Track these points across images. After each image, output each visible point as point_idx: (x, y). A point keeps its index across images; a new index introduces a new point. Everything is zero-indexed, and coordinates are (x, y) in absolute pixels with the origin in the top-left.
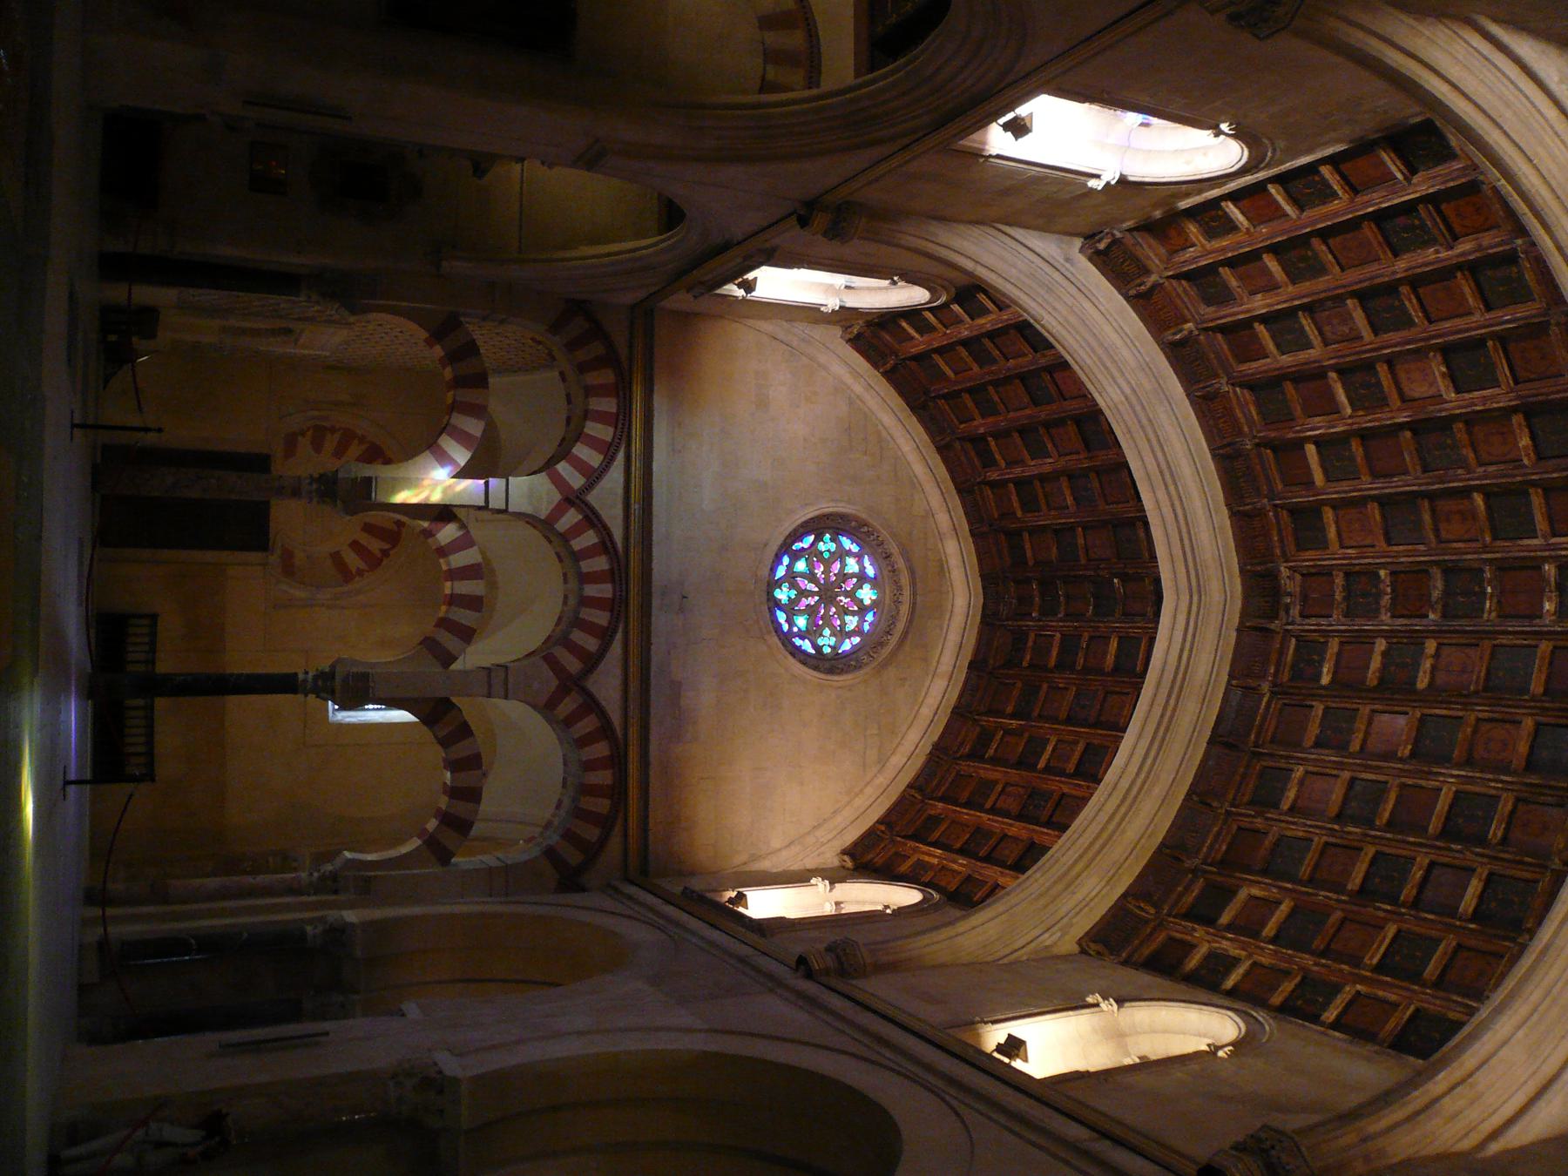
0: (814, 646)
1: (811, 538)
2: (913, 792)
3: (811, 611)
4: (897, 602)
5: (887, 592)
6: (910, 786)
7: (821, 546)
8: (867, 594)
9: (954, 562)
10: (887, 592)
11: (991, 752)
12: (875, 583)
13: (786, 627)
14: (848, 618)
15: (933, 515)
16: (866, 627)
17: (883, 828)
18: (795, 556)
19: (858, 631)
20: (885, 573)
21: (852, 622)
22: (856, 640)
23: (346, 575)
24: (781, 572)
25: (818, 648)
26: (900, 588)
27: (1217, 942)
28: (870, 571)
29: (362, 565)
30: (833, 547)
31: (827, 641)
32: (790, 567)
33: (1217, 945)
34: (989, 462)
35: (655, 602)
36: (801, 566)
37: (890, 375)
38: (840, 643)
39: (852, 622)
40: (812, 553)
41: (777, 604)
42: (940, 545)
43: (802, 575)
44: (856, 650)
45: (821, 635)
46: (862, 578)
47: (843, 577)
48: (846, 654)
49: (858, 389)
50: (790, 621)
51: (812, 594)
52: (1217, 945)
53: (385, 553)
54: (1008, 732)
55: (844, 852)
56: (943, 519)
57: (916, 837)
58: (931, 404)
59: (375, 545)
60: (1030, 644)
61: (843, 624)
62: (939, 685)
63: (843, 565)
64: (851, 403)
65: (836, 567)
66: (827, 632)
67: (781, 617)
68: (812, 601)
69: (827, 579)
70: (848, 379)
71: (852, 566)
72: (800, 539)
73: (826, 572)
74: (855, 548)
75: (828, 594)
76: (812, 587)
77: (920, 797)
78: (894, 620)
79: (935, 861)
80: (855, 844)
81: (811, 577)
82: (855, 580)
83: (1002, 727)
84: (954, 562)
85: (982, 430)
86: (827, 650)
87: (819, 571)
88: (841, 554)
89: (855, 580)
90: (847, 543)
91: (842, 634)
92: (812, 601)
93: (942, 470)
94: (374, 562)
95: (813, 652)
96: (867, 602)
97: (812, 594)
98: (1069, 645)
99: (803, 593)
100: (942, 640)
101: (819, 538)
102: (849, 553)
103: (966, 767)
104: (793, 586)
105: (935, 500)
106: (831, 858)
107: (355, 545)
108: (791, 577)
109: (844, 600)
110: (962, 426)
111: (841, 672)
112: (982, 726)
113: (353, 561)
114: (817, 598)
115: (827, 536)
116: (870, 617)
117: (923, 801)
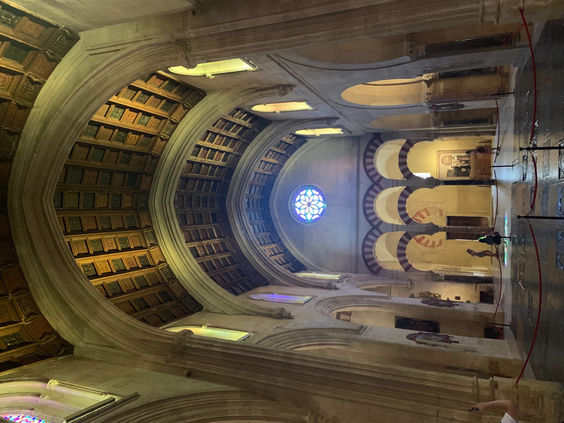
9: (276, 213)
11: (271, 166)
16: (299, 196)
22: (301, 193)
23: (425, 210)
28: (297, 210)
29: (421, 212)
34: (270, 236)
53: (416, 216)
54: (267, 170)
55: (307, 141)
56: (279, 223)
57: (290, 145)
59: (418, 217)
62: (281, 182)
64: (304, 252)
74: (302, 216)
78: (292, 199)
79: (288, 140)
80: (304, 143)
83: (268, 172)
84: (276, 213)
93: (280, 235)
94: (418, 213)
103: (276, 162)
105: (281, 228)
106: (310, 141)
107: (423, 218)
113: (424, 213)
114: (312, 203)
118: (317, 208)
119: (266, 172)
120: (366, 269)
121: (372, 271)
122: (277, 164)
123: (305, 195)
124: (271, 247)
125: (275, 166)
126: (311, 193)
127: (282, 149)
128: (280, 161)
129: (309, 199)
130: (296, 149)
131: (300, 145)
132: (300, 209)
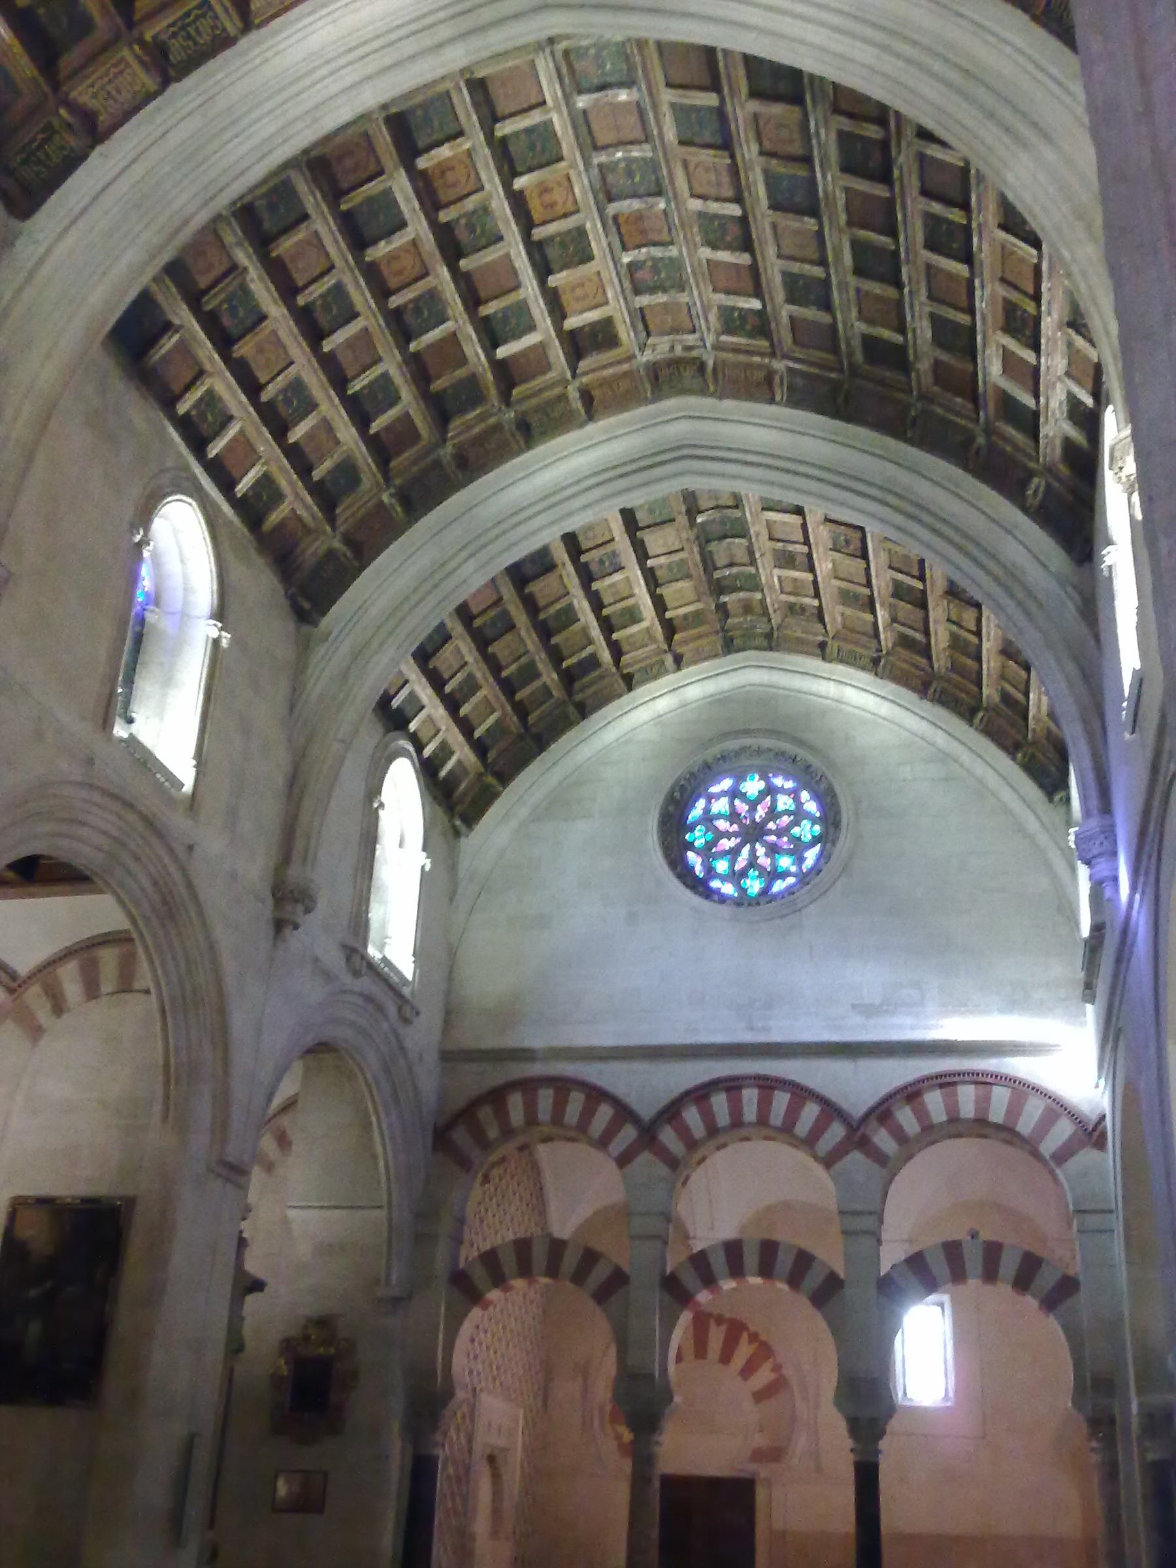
0: (812, 844)
1: (691, 855)
2: (977, 721)
3: (773, 850)
4: (759, 751)
5: (748, 763)
6: (970, 722)
7: (699, 843)
8: (753, 786)
10: (748, 763)
11: (919, 636)
12: (740, 778)
13: (791, 880)
14: (781, 807)
15: (660, 716)
16: (789, 785)
17: (1019, 755)
18: (710, 872)
19: (794, 794)
20: (726, 766)
21: (784, 802)
22: (805, 795)
24: (728, 889)
25: (816, 840)
26: (743, 749)
27: (1053, 413)
28: (726, 784)
30: (699, 830)
31: (806, 831)
32: (724, 879)
33: (1057, 412)
35: (762, 1038)
36: (722, 866)
37: (505, 778)
38: (808, 816)
39: (784, 802)
40: (707, 852)
41: (765, 892)
42: (694, 705)
43: (733, 863)
44: (816, 796)
45: (799, 839)
46: (734, 793)
47: (734, 816)
48: (822, 806)
49: (523, 812)
50: (784, 875)
51: (753, 851)
52: (1057, 412)
54: (894, 620)
55: (1051, 800)
58: (534, 730)
60: (792, 599)
61: (787, 812)
63: (719, 816)
65: (722, 825)
66: (796, 831)
67: (779, 886)
68: (761, 850)
69: (735, 834)
70: (513, 823)
71: (721, 806)
72: (691, 870)
73: (728, 835)
74: (701, 804)
75: (753, 833)
76: (745, 851)
77: (980, 714)
78: (780, 755)
80: (1041, 786)
81: (734, 853)
82: (737, 802)
84: (710, 687)
85: (555, 676)
86: (817, 829)
87: (726, 844)
88: (708, 819)
89: (737, 802)
90: (696, 812)
91: (798, 815)
92: (761, 850)
95: (818, 847)
96: (762, 785)
97: (753, 851)
98: (786, 560)
99: (753, 863)
100: (799, 695)
101: (690, 846)
102: (707, 810)
104: (743, 874)
108: (736, 877)
109: (761, 812)
110: (554, 693)
111: (838, 812)
112: (895, 645)
114: (758, 845)
115: (688, 837)
116: (778, 781)
117: (986, 709)
118: (737, 867)
119: (882, 614)
120: (459, 1102)
121: (450, 1125)
122: (932, 667)
123: (798, 815)
124: (540, 666)
125: (923, 662)
126: (807, 838)
127: (1003, 677)
128: (949, 681)
129: (779, 833)
130: (1012, 748)
131: (1033, 769)
132: (734, 793)
